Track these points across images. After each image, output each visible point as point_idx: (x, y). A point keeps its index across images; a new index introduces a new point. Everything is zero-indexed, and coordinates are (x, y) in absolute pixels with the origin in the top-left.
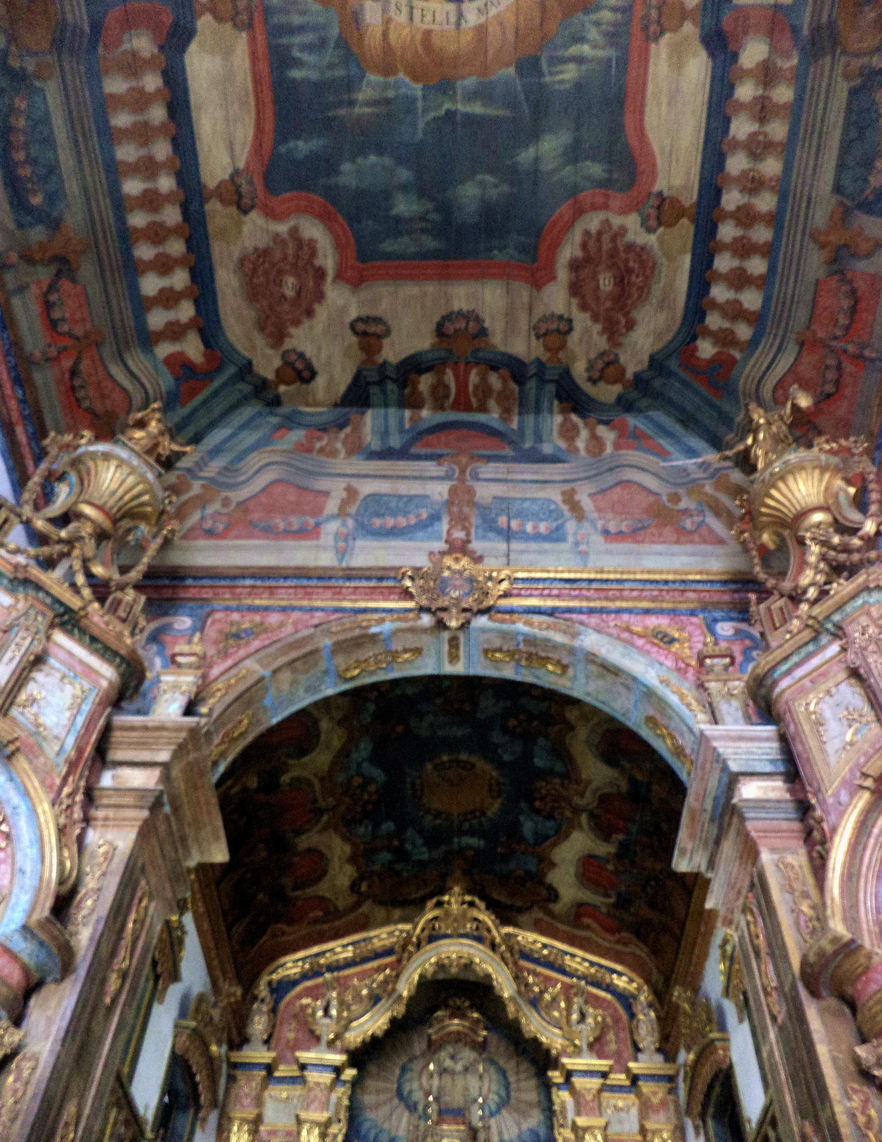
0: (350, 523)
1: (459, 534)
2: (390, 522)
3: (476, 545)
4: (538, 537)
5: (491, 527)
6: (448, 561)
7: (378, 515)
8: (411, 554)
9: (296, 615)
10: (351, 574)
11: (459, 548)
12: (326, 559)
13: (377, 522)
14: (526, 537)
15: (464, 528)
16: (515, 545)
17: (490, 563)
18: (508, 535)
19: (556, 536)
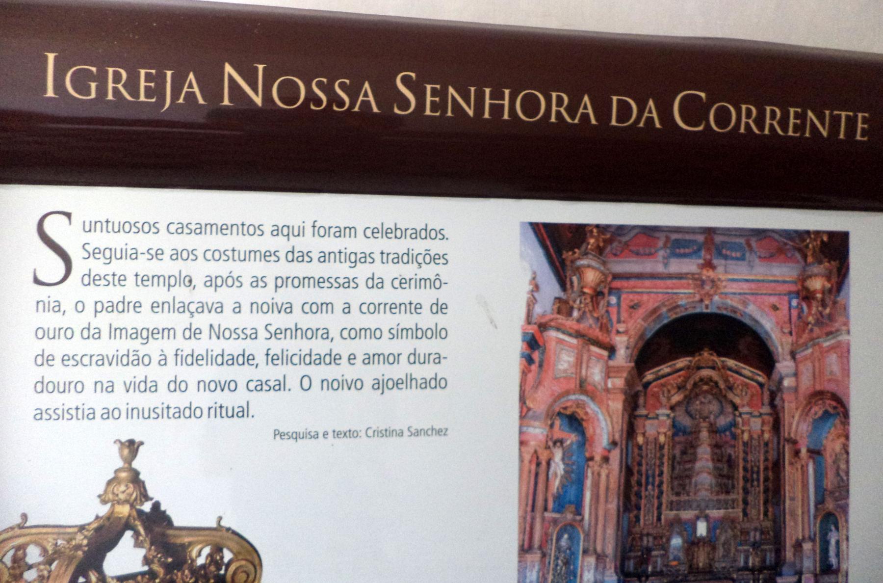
0: (668, 251)
1: (708, 257)
2: (682, 251)
3: (715, 262)
4: (737, 259)
5: (720, 254)
6: (705, 272)
7: (679, 248)
8: (690, 266)
9: (652, 295)
10: (670, 277)
11: (709, 265)
12: (660, 269)
13: (678, 250)
14: (732, 258)
15: (711, 255)
16: (729, 262)
17: (720, 269)
18: (726, 257)
19: (742, 258)
